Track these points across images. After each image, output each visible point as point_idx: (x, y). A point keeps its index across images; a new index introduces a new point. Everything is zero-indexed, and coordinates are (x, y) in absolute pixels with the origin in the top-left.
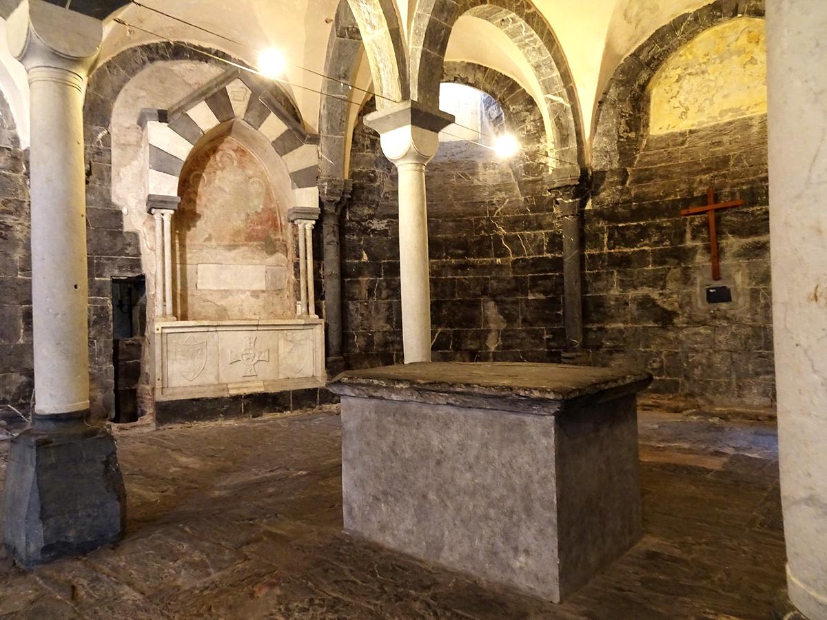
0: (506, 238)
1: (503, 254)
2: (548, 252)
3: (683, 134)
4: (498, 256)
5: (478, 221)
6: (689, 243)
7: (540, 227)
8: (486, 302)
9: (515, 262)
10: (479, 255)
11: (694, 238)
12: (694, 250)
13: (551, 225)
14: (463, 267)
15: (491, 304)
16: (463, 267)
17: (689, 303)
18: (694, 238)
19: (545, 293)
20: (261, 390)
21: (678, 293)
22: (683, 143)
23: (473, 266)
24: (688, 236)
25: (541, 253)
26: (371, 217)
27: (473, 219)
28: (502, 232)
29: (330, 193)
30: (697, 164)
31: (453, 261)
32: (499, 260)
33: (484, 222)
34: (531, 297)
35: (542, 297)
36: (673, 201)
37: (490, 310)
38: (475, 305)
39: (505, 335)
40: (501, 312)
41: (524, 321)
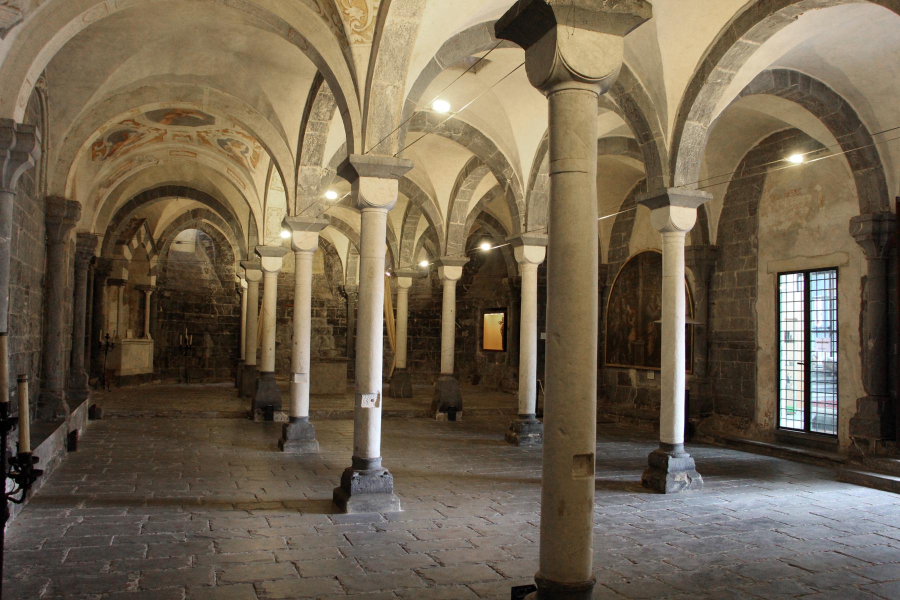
0: (216, 306)
1: (214, 313)
2: (233, 314)
3: (283, 273)
4: (212, 314)
5: (205, 296)
6: (286, 317)
7: (230, 303)
8: (206, 334)
9: (219, 317)
10: (205, 312)
11: (288, 315)
12: (288, 319)
13: (234, 303)
14: (198, 318)
15: (209, 335)
16: (198, 318)
17: (285, 340)
18: (288, 315)
19: (230, 332)
20: (140, 372)
21: (281, 336)
22: (283, 277)
23: (203, 318)
24: (286, 314)
25: (230, 314)
26: (165, 290)
27: (204, 295)
28: (215, 302)
29: (160, 279)
30: (289, 287)
31: (195, 314)
32: (212, 316)
33: (208, 298)
34: (224, 333)
35: (228, 333)
36: (282, 300)
37: (208, 338)
38: (202, 335)
39: (213, 350)
40: (212, 339)
41: (222, 344)
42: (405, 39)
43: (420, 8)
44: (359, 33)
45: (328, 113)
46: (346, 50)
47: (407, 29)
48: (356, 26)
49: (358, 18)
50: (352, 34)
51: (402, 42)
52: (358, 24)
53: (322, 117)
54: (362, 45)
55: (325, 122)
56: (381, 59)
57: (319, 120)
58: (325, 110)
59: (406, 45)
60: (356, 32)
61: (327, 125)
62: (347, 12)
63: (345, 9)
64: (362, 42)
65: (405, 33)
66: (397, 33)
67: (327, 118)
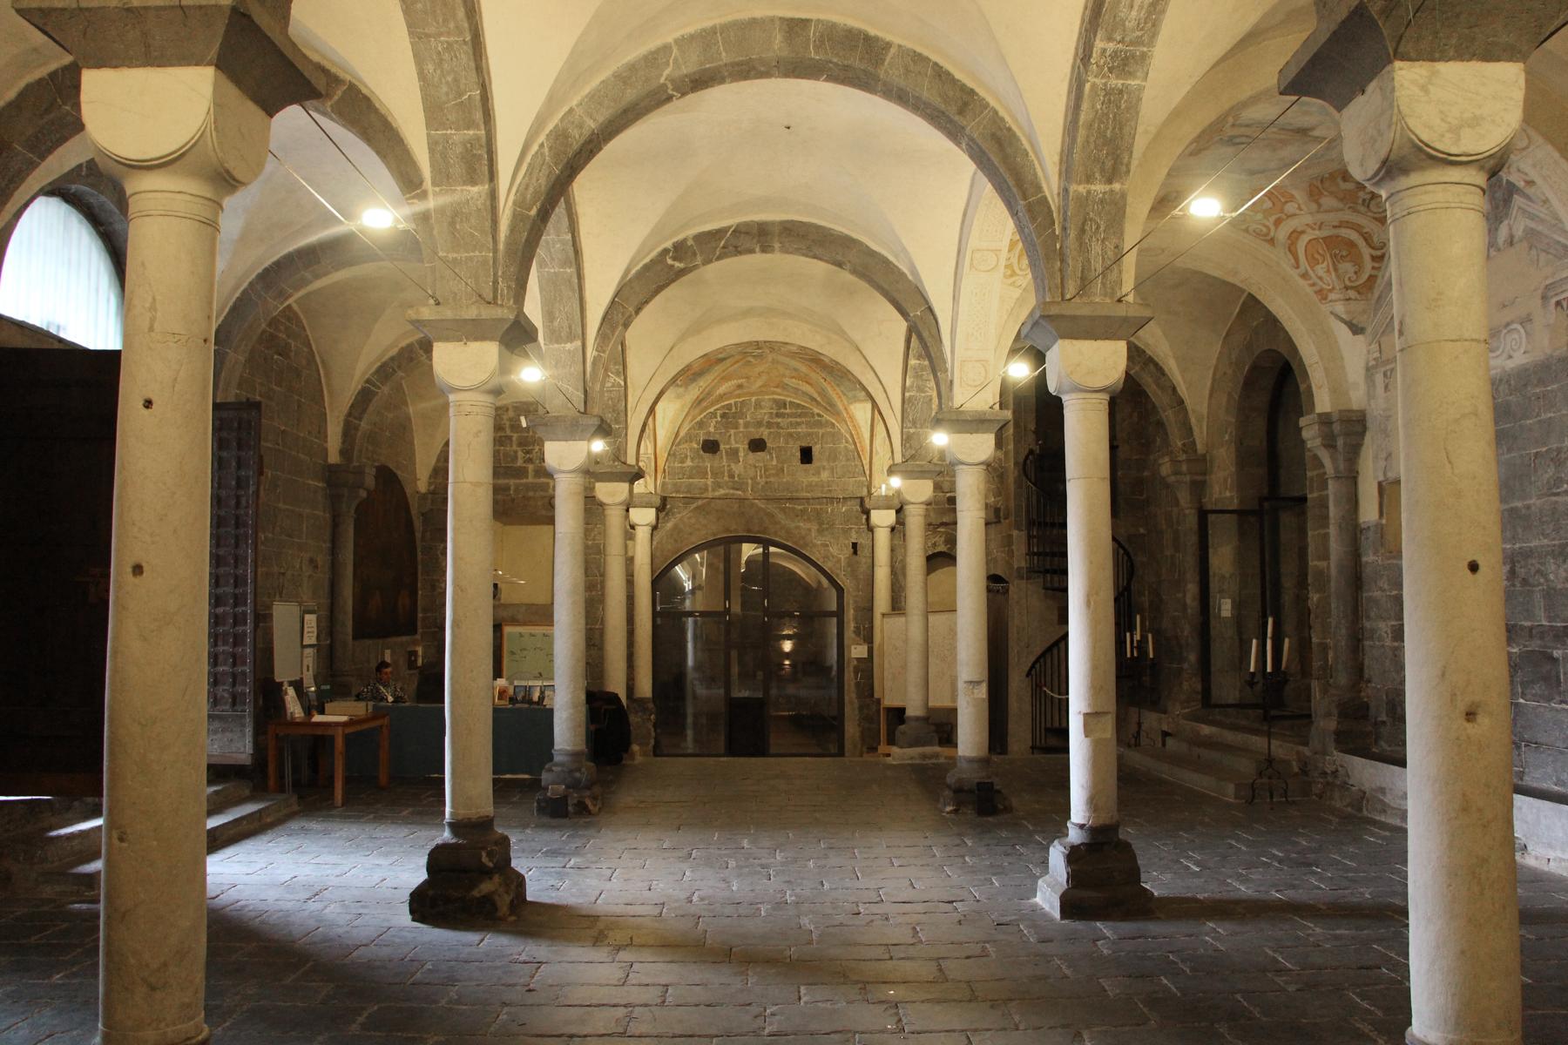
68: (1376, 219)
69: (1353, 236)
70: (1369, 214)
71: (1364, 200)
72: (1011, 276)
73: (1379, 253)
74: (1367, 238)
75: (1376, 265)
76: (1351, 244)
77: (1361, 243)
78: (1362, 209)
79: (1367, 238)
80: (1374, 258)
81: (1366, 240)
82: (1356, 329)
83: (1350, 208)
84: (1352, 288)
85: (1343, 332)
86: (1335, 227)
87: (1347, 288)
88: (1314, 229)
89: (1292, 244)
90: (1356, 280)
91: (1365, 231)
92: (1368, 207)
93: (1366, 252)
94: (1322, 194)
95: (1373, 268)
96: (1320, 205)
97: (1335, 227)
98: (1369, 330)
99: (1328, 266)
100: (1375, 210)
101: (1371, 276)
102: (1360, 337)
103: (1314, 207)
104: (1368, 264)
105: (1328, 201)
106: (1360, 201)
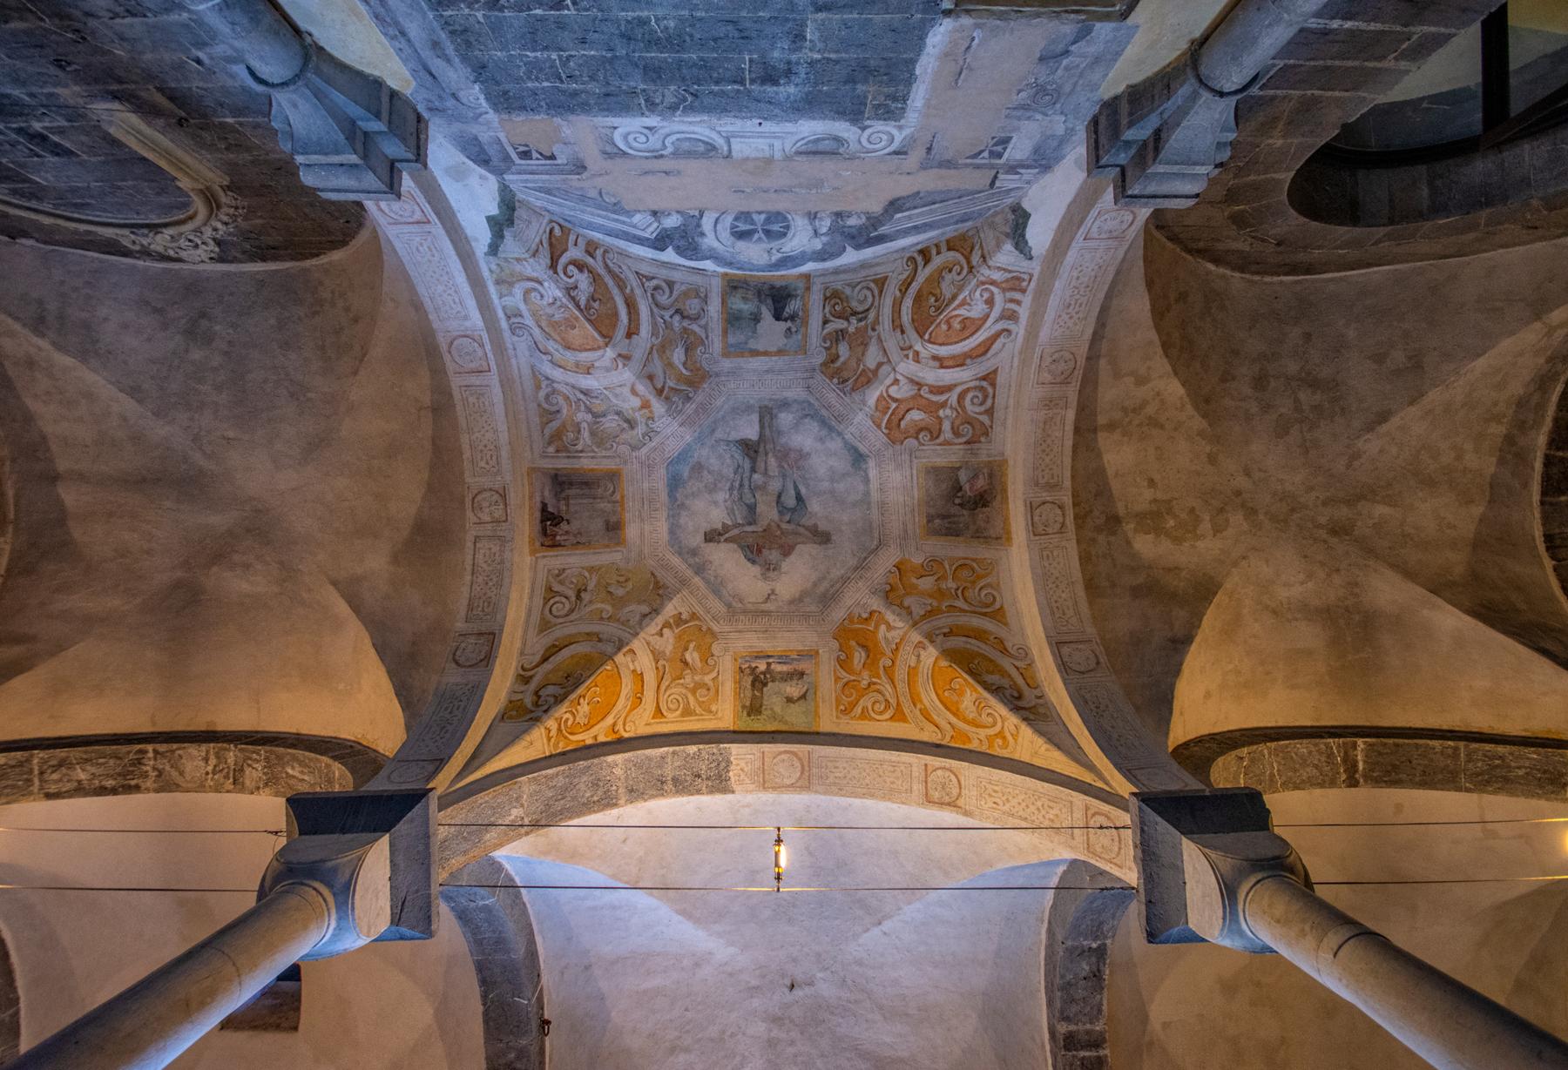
42: (592, 796)
43: (643, 794)
44: (559, 730)
45: (69, 786)
46: (506, 727)
47: (608, 791)
48: (567, 720)
49: (578, 720)
50: (556, 719)
51: (588, 795)
52: (570, 723)
53: (55, 776)
54: (545, 741)
55: (35, 788)
56: (557, 775)
57: (42, 773)
58: (82, 776)
59: (584, 804)
60: (560, 725)
61: (31, 793)
62: (582, 700)
63: (584, 697)
64: (549, 739)
65: (600, 793)
66: (599, 780)
67: (53, 789)
68: (881, 292)
69: (908, 303)
70: (876, 304)
71: (860, 320)
72: (1004, 738)
73: (919, 259)
74: (907, 285)
75: (934, 252)
76: (918, 299)
77: (915, 286)
78: (872, 315)
79: (907, 285)
80: (927, 261)
81: (906, 289)
82: (1020, 217)
83: (873, 330)
84: (969, 262)
85: (1039, 234)
86: (903, 332)
87: (971, 268)
88: (917, 353)
89: (971, 357)
90: (959, 263)
91: (898, 293)
92: (868, 310)
93: (923, 275)
94: (863, 370)
95: (938, 253)
96: (880, 365)
97: (903, 332)
98: (1009, 201)
99: (955, 309)
100: (870, 299)
101: (949, 249)
102: (1026, 205)
103: (885, 369)
104: (937, 261)
105: (872, 358)
106: (863, 323)
